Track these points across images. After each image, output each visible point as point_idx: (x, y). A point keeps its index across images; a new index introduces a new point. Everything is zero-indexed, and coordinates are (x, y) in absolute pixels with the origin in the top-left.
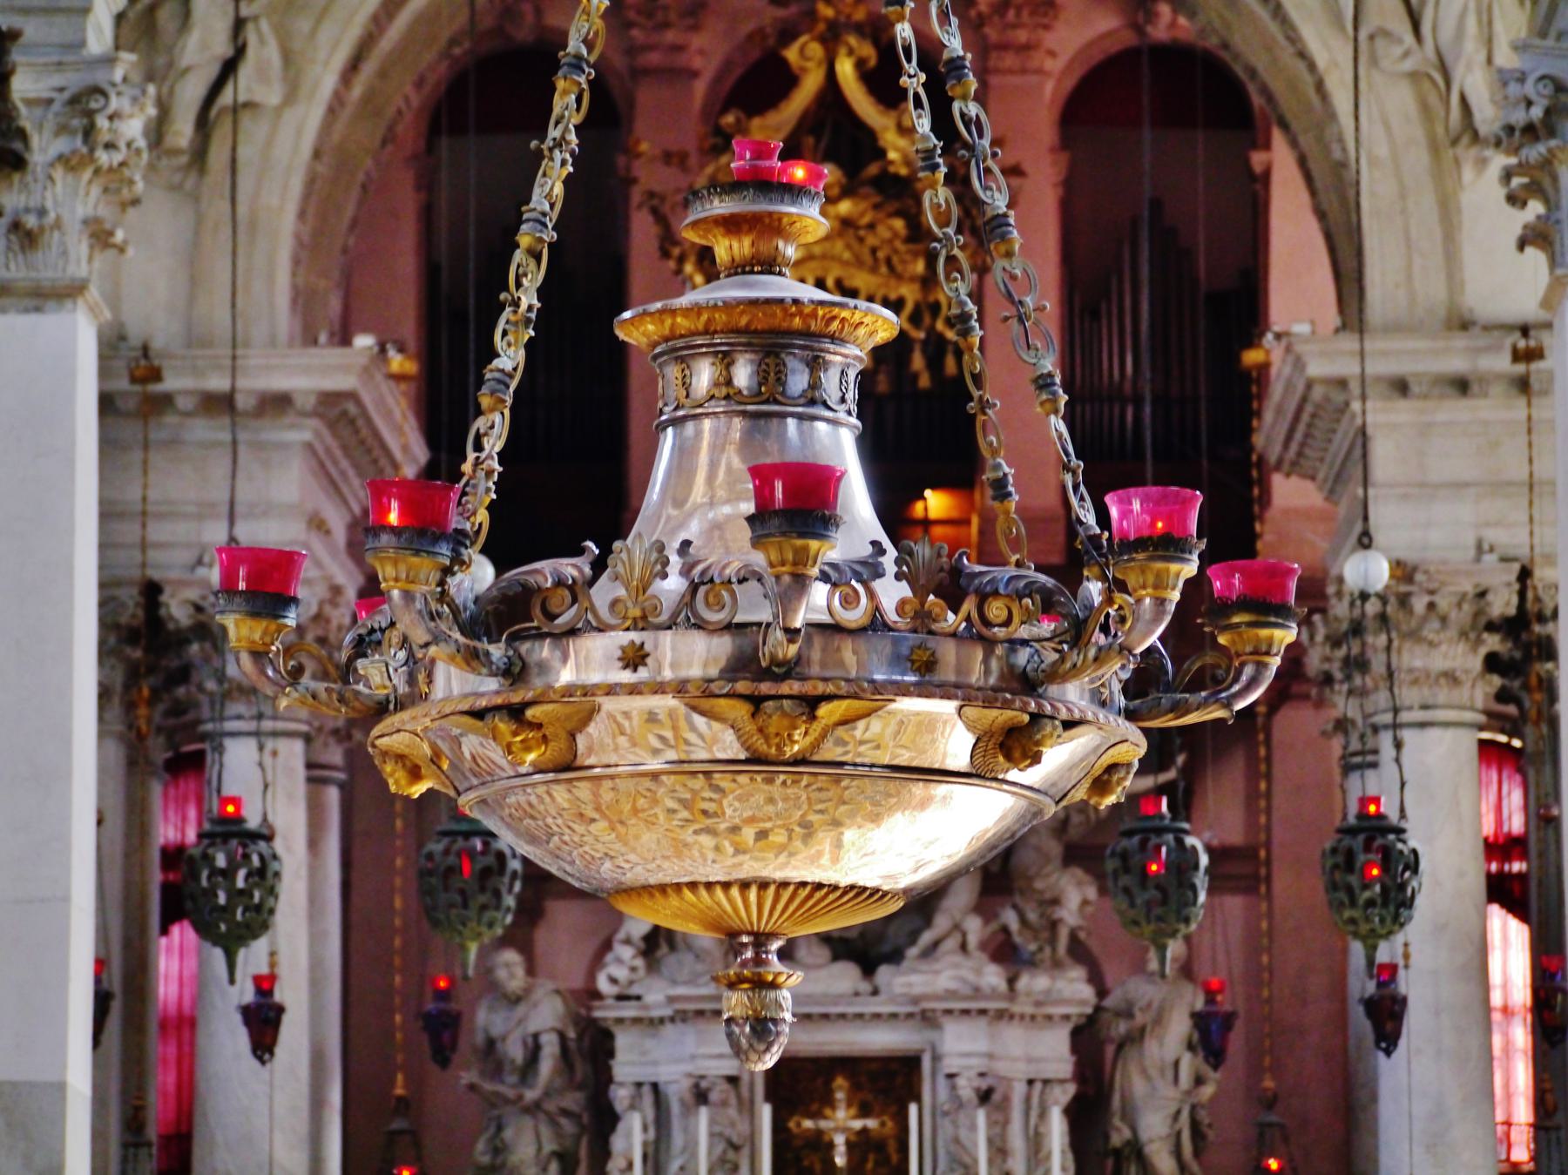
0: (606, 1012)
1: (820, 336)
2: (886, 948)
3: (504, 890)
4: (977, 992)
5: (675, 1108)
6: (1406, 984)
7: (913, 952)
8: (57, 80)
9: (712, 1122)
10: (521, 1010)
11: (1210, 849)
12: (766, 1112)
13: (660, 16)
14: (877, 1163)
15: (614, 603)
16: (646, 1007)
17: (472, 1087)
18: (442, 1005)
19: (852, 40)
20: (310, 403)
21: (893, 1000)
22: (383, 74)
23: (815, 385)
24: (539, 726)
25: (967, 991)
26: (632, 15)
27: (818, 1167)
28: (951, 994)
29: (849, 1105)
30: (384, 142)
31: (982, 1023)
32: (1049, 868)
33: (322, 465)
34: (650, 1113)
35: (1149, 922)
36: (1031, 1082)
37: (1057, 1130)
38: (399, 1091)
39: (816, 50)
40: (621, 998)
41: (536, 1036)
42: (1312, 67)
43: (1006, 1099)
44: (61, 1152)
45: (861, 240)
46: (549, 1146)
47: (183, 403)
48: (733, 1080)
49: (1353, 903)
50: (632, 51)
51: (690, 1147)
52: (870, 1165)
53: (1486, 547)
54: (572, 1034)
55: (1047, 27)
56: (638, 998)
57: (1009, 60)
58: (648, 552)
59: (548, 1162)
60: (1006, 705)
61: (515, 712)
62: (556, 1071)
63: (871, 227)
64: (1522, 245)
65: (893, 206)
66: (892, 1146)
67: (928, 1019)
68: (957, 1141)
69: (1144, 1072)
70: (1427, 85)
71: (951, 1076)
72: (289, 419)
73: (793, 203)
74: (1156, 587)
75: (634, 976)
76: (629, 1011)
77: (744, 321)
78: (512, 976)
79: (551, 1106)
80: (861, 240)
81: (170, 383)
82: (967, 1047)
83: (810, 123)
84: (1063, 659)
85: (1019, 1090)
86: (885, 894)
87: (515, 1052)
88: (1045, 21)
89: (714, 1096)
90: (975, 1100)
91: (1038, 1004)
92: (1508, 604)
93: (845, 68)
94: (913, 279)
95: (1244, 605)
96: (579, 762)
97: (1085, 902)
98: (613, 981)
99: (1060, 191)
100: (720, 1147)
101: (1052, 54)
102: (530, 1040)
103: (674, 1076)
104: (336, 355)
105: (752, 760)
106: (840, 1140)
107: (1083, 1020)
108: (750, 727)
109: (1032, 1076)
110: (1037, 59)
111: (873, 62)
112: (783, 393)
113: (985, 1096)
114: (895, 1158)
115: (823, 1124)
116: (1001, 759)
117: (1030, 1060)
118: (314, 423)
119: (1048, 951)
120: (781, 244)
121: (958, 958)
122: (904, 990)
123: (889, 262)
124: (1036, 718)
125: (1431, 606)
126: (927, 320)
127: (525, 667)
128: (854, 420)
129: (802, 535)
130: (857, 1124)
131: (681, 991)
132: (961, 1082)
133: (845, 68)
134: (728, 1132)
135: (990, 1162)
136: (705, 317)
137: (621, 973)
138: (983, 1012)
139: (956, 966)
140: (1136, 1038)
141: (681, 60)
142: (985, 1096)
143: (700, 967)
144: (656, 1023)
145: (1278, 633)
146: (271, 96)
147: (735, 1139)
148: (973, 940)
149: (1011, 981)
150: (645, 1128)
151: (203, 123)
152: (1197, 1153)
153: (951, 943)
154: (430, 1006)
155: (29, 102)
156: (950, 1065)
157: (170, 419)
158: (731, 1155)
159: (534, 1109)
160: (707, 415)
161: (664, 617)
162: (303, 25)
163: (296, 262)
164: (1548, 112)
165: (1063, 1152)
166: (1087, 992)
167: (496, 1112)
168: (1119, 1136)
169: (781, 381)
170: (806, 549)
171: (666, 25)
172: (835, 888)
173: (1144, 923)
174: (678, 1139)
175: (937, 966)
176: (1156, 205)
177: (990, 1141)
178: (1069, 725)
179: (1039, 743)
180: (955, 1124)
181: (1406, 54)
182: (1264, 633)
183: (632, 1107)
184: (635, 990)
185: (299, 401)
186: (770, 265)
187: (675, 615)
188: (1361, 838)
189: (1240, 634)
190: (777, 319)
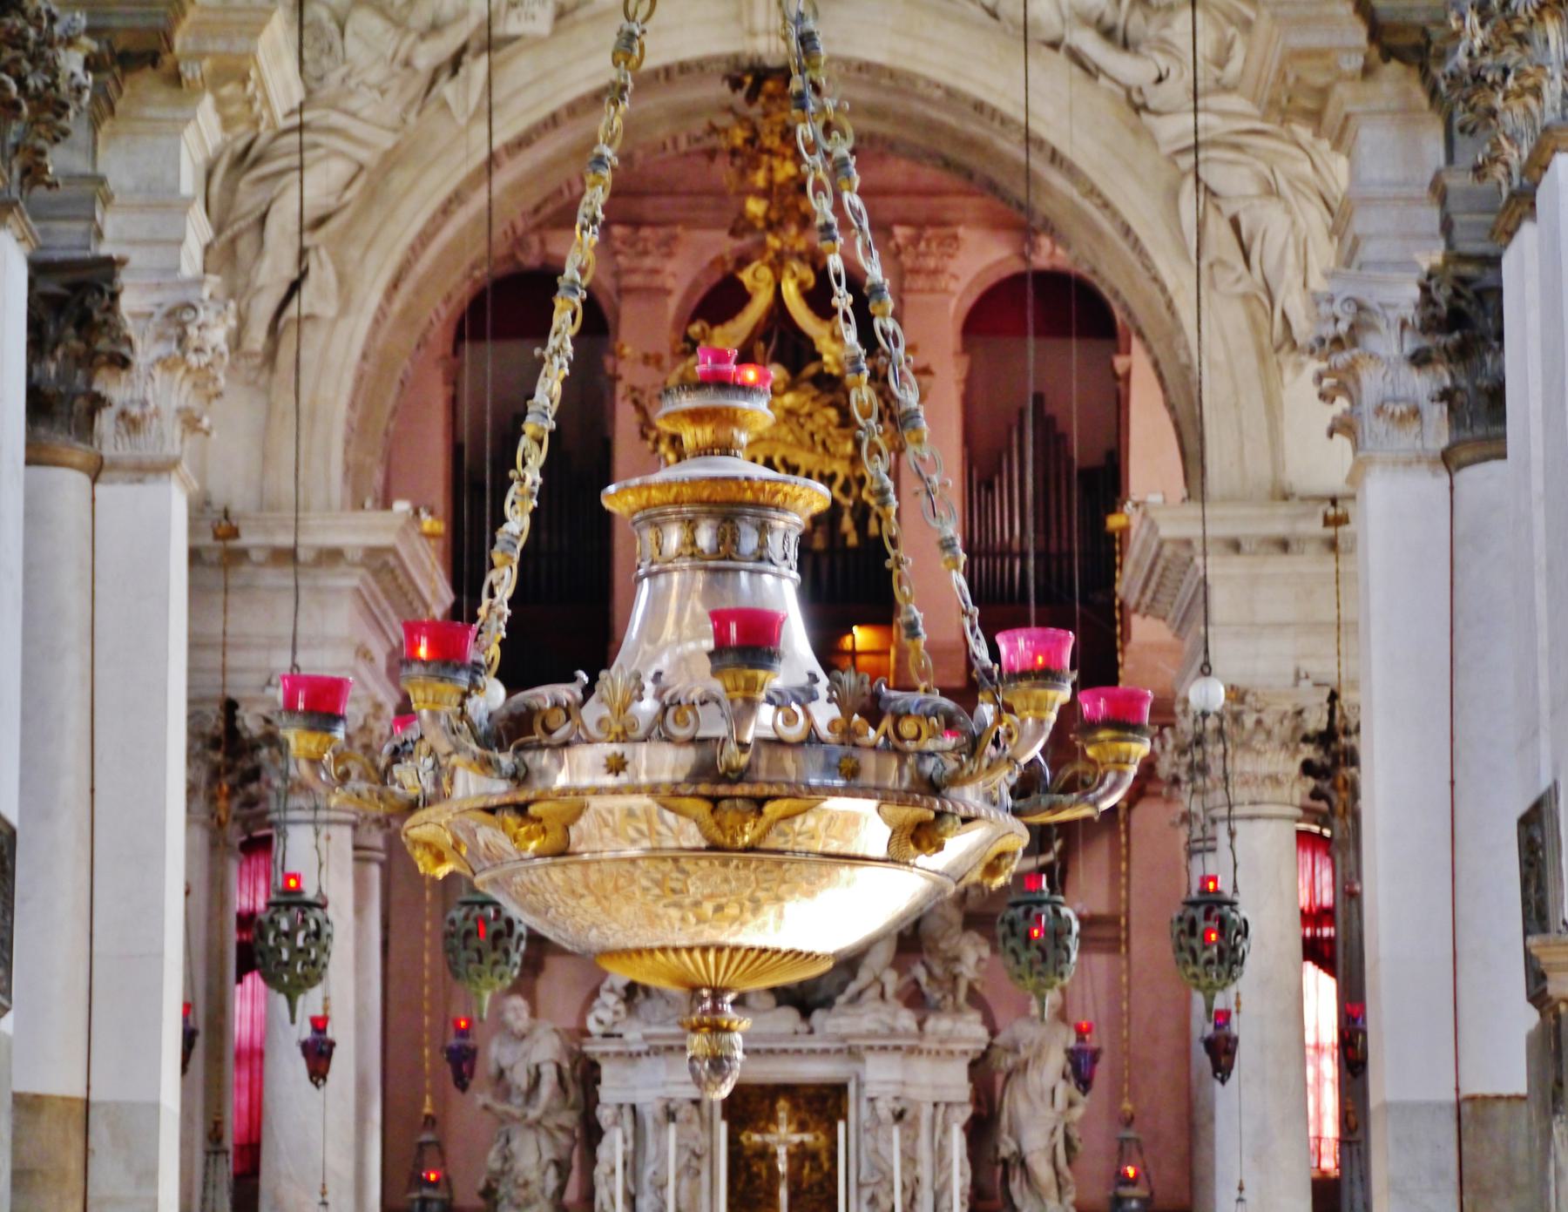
0: (593, 1048)
1: (767, 506)
2: (820, 996)
3: (512, 950)
4: (893, 1032)
5: (650, 1125)
6: (1237, 1026)
7: (841, 999)
8: (157, 297)
9: (679, 1136)
10: (526, 1044)
11: (1080, 918)
12: (722, 1128)
13: (640, 246)
14: (812, 1169)
15: (600, 722)
16: (627, 1043)
17: (486, 1108)
18: (462, 1041)
19: (795, 265)
20: (358, 556)
21: (825, 1038)
22: (418, 292)
23: (763, 545)
24: (540, 820)
25: (885, 1031)
26: (617, 244)
27: (764, 1173)
28: (872, 1034)
29: (790, 1122)
30: (418, 347)
31: (897, 1056)
32: (951, 932)
33: (366, 604)
35: (1031, 975)
36: (936, 1105)
37: (957, 1143)
38: (427, 1110)
39: (766, 273)
40: (606, 1035)
42: (1163, 289)
43: (916, 1118)
44: (156, 1159)
45: (802, 426)
46: (548, 1155)
47: (256, 556)
48: (696, 1103)
49: (1195, 961)
50: (617, 274)
51: (662, 1156)
52: (806, 1171)
53: (1303, 675)
55: (951, 256)
56: (620, 1036)
57: (921, 282)
58: (627, 682)
59: (547, 1167)
60: (916, 804)
61: (521, 809)
62: (553, 1096)
63: (810, 415)
64: (1331, 433)
65: (828, 398)
66: (824, 1157)
67: (853, 1054)
68: (876, 1151)
69: (1027, 1096)
70: (1255, 304)
71: (872, 1100)
72: (342, 568)
73: (745, 399)
74: (1037, 709)
75: (617, 1019)
76: (612, 1046)
77: (705, 494)
78: (518, 1017)
79: (550, 1122)
80: (802, 426)
81: (245, 540)
82: (883, 1076)
83: (762, 332)
84: (962, 766)
85: (927, 1111)
86: (817, 957)
87: (521, 1079)
88: (951, 251)
89: (681, 1115)
90: (891, 1118)
91: (942, 1042)
92: (1320, 720)
93: (790, 289)
94: (843, 457)
95: (1109, 724)
96: (571, 849)
97: (980, 960)
98: (600, 1022)
99: (962, 387)
100: (686, 1156)
101: (955, 277)
102: (533, 1071)
103: (649, 1100)
104: (380, 517)
105: (714, 847)
106: (782, 1152)
107: (978, 1055)
108: (709, 821)
109: (937, 1099)
110: (943, 281)
111: (811, 283)
112: (738, 552)
113: (899, 1116)
114: (826, 1166)
115: (769, 1138)
116: (912, 847)
117: (935, 1087)
118: (361, 571)
119: (950, 999)
120: (736, 432)
121: (878, 1004)
122: (835, 1030)
123: (824, 444)
124: (940, 815)
125: (1259, 722)
126: (855, 490)
127: (528, 772)
128: (795, 574)
129: (752, 666)
130: (796, 1138)
131: (655, 1030)
132: (880, 1104)
133: (790, 289)
134: (692, 1144)
135: (903, 1168)
136: (674, 490)
137: (607, 1016)
138: (897, 1048)
139: (877, 1011)
140: (1021, 1069)
141: (657, 281)
142: (899, 1116)
143: (670, 1012)
145: (1135, 747)
146: (328, 309)
147: (698, 1150)
149: (921, 1024)
150: (625, 1141)
151: (274, 330)
152: (1069, 1162)
153: (873, 992)
154: (453, 1041)
155: (135, 316)
156: (870, 1090)
157: (246, 569)
158: (694, 1163)
159: (537, 1124)
160: (675, 569)
161: (641, 733)
162: (354, 253)
163: (347, 442)
164: (1352, 327)
165: (961, 1161)
166: (981, 1032)
167: (504, 1128)
168: (1006, 1148)
169: (735, 541)
170: (755, 679)
171: (645, 253)
172: (777, 952)
173: (1027, 977)
174: (651, 1150)
175: (861, 1011)
176: (1039, 399)
177: (903, 1152)
178: (966, 820)
179: (942, 835)
180: (875, 1139)
181: (1239, 280)
182: (1124, 746)
183: (615, 1123)
184: (617, 1030)
185: (349, 555)
186: (726, 449)
187: (650, 730)
188: (1202, 909)
189: (1104, 748)
190: (733, 493)
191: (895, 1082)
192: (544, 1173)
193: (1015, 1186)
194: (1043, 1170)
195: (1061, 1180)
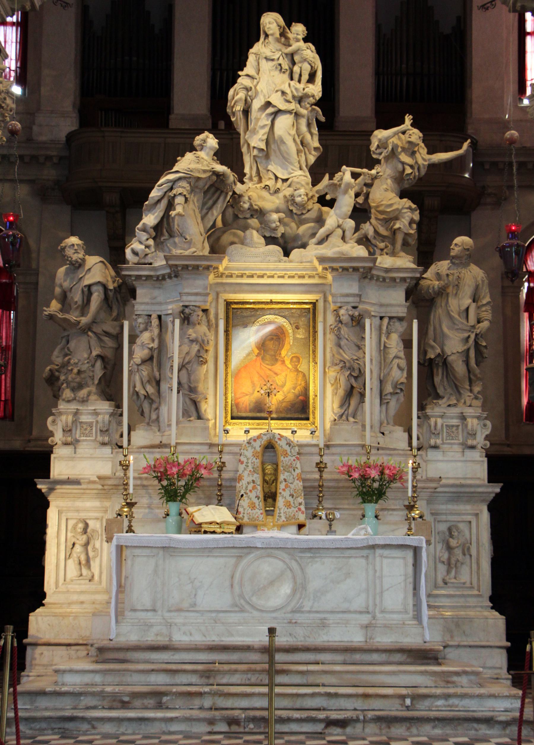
31: (356, 276)
34: (156, 331)
36: (381, 318)
41: (89, 286)
46: (94, 353)
48: (205, 311)
54: (111, 286)
56: (151, 264)
59: (96, 361)
62: (100, 309)
87: (77, 297)
89: (194, 318)
102: (86, 289)
117: (381, 305)
144: (161, 279)
148: (348, 234)
150: (153, 340)
152: (478, 364)
167: (66, 334)
191: (354, 295)
192: (93, 366)
193: (437, 380)
194: (460, 368)
195: (472, 376)
